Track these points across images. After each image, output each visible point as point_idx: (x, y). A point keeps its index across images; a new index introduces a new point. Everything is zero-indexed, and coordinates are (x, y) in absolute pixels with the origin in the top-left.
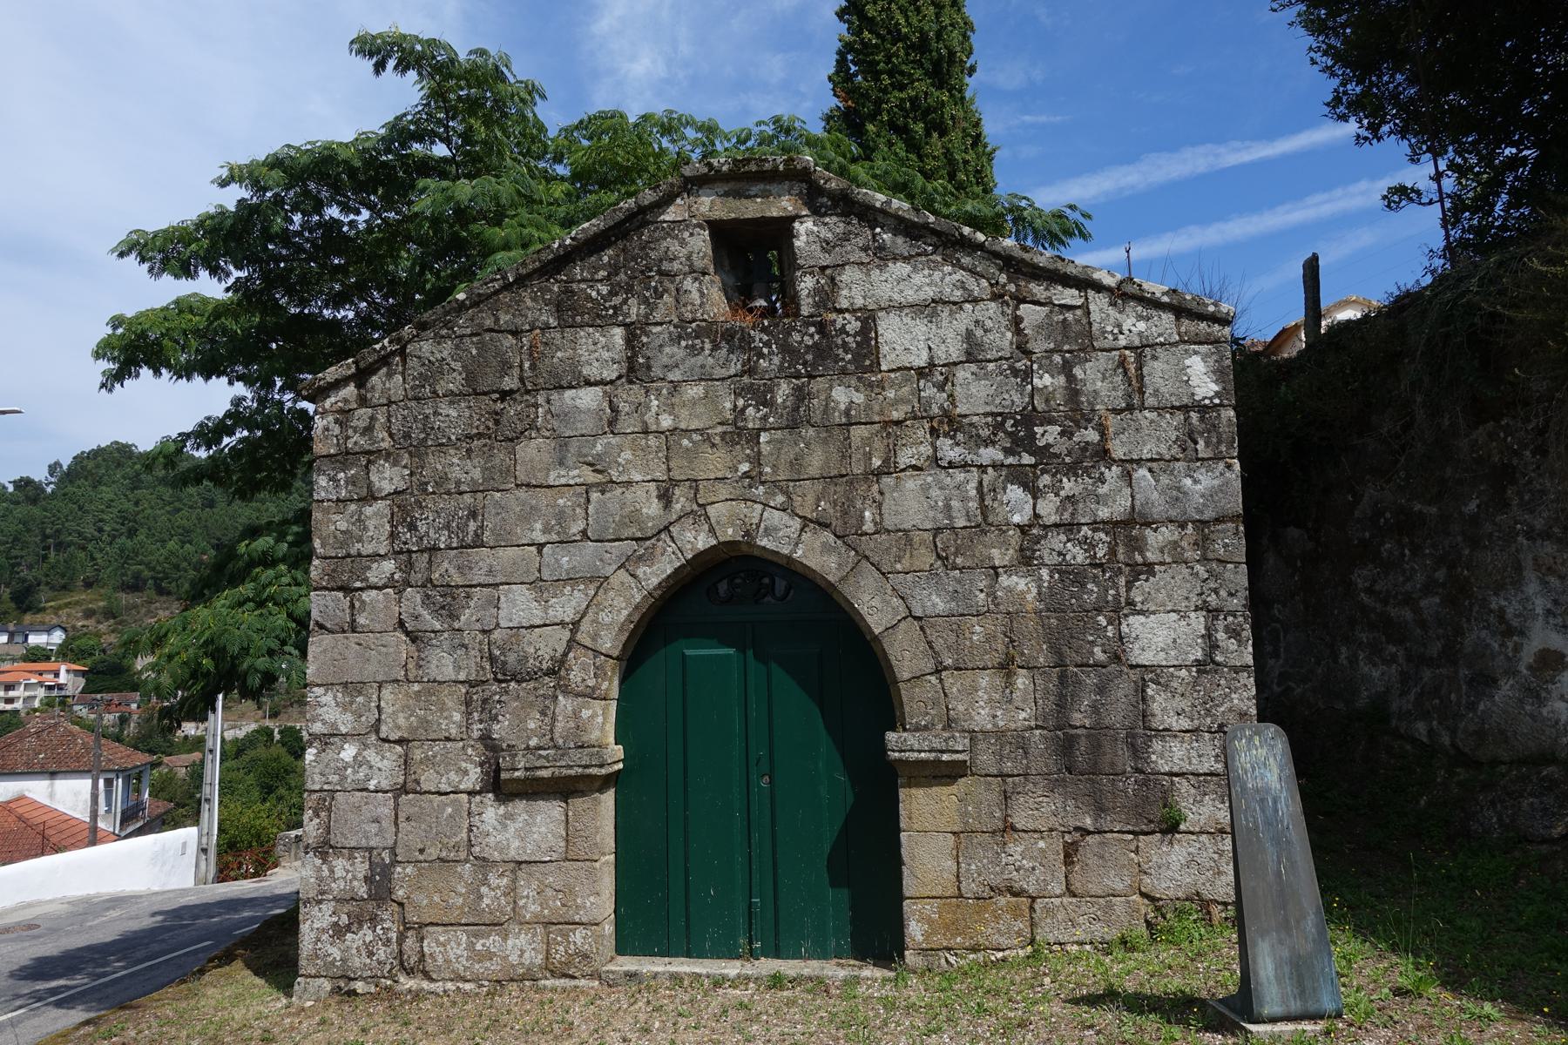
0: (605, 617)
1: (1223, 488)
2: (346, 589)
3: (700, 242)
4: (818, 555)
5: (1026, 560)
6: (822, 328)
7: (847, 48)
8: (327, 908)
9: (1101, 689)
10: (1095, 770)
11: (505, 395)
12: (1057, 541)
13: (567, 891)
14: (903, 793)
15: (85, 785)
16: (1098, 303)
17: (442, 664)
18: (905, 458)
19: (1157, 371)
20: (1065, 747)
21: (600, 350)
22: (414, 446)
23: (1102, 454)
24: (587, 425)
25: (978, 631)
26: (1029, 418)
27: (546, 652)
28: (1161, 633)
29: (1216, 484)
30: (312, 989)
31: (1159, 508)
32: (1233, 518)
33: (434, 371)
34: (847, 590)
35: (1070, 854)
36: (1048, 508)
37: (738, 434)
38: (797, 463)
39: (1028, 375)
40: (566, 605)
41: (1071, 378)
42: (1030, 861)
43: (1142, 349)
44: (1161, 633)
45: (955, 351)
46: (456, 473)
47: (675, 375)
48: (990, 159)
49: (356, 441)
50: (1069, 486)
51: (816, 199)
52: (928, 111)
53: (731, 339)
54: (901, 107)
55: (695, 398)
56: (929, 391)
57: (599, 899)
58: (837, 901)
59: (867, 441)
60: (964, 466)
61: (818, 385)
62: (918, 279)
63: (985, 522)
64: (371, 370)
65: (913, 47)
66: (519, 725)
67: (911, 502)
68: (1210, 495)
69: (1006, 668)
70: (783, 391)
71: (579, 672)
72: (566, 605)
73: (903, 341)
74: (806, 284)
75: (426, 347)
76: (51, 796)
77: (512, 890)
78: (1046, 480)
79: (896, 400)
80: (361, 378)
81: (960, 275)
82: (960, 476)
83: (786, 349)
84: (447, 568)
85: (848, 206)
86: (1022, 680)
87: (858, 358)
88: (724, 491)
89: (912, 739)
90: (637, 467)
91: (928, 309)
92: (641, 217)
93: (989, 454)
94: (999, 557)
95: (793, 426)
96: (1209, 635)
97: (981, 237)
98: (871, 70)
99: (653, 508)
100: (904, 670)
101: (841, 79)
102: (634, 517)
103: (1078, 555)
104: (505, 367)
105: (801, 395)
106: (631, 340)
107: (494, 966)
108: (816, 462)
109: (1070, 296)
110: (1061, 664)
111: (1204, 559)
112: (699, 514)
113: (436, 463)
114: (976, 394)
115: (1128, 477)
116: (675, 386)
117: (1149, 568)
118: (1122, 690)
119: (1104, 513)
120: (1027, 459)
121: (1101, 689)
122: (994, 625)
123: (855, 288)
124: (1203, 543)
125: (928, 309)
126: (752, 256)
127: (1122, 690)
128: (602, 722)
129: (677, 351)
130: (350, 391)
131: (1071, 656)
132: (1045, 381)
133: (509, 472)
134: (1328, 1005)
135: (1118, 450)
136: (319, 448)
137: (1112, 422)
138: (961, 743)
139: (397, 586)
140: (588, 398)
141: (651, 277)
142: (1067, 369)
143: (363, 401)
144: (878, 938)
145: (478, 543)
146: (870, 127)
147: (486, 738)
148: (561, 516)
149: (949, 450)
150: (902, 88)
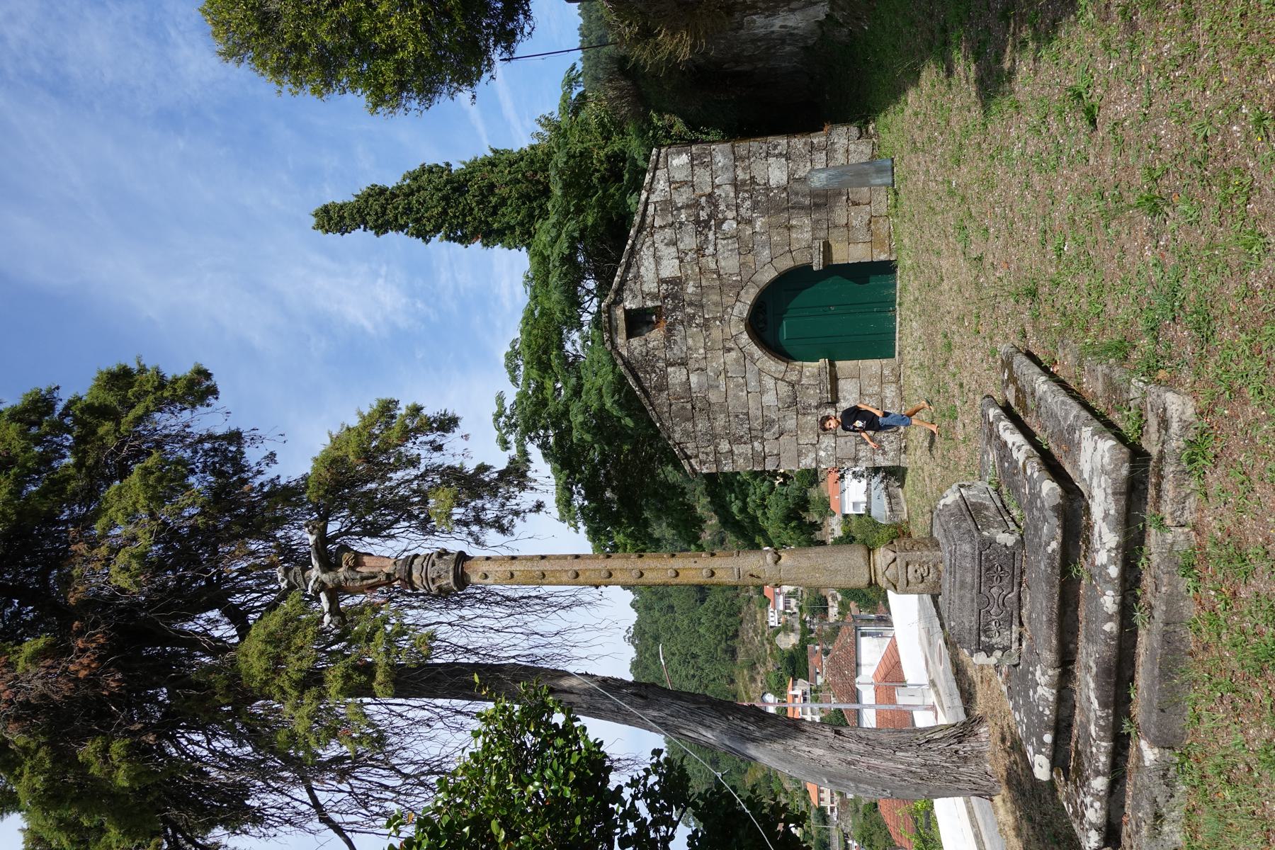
0: (773, 369)
1: (722, 152)
2: (764, 458)
3: (635, 342)
4: (749, 296)
5: (750, 222)
6: (665, 298)
7: (448, 238)
8: (876, 457)
9: (797, 194)
10: (826, 196)
11: (693, 408)
12: (742, 211)
13: (870, 377)
14: (835, 263)
15: (865, 643)
16: (653, 198)
17: (791, 423)
18: (713, 266)
19: (679, 176)
20: (817, 206)
21: (676, 376)
22: (713, 437)
23: (710, 196)
24: (704, 379)
25: (776, 238)
26: (697, 222)
27: (786, 389)
28: (776, 173)
29: (721, 154)
30: (905, 461)
31: (730, 175)
32: (733, 146)
33: (686, 433)
34: (762, 285)
35: (856, 204)
36: (731, 214)
37: (706, 325)
38: (716, 304)
39: (681, 223)
40: (769, 382)
41: (682, 208)
42: (858, 218)
43: (670, 182)
44: (776, 173)
45: (673, 249)
46: (722, 423)
47: (685, 349)
48: (495, 151)
49: (711, 458)
50: (722, 207)
51: (618, 301)
52: (482, 194)
53: (670, 330)
54: (483, 210)
55: (692, 341)
56: (688, 258)
57: (873, 365)
58: (874, 281)
59: (707, 279)
60: (716, 245)
61: (687, 298)
62: (646, 264)
63: (737, 237)
64: (685, 454)
65: (447, 204)
66: (812, 397)
67: (729, 263)
68: (725, 156)
69: (789, 228)
70: (690, 310)
71: (793, 377)
72: (769, 382)
73: (670, 268)
74: (649, 304)
75: (677, 436)
76: (871, 665)
77: (870, 396)
78: (720, 216)
79: (693, 270)
80: (688, 458)
81: (644, 248)
82: (719, 246)
83: (674, 310)
84: (756, 424)
85: (619, 291)
86: (794, 222)
87: (676, 284)
88: (726, 330)
89: (815, 261)
90: (720, 360)
91: (657, 260)
92: (627, 364)
93: (711, 236)
94: (749, 232)
95: (702, 306)
96: (777, 156)
97: (630, 242)
98: (462, 226)
99: (733, 354)
100: (791, 264)
101: (465, 240)
102: (737, 361)
103: (748, 203)
104: (683, 408)
105: (691, 304)
106: (672, 365)
107: (896, 400)
108: (715, 298)
109: (651, 209)
110: (788, 209)
111: (749, 158)
112: (735, 338)
113: (719, 430)
114: (689, 241)
115: (718, 186)
116: (688, 348)
117: (752, 178)
118: (797, 187)
119: (732, 195)
120: (713, 222)
121: (797, 194)
122: (774, 233)
123: (650, 286)
124: (742, 159)
125: (657, 260)
126: (638, 322)
127: (797, 187)
128: (811, 368)
129: (676, 348)
130: (693, 461)
131: (785, 205)
132: (683, 216)
133: (721, 405)
134: (889, 163)
135: (709, 190)
136: (714, 470)
137: (698, 192)
138: (816, 244)
139: (763, 440)
140: (694, 379)
141: (649, 360)
142: (678, 209)
143: (697, 456)
144: (887, 268)
145: (747, 414)
146: (495, 226)
147: (817, 408)
148: (737, 386)
149: (711, 250)
150: (472, 209)
